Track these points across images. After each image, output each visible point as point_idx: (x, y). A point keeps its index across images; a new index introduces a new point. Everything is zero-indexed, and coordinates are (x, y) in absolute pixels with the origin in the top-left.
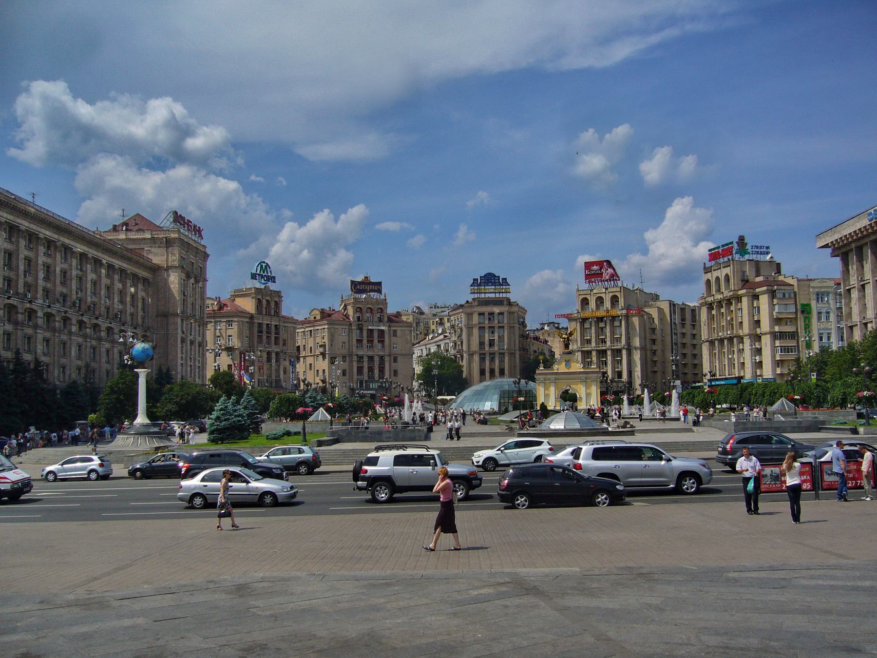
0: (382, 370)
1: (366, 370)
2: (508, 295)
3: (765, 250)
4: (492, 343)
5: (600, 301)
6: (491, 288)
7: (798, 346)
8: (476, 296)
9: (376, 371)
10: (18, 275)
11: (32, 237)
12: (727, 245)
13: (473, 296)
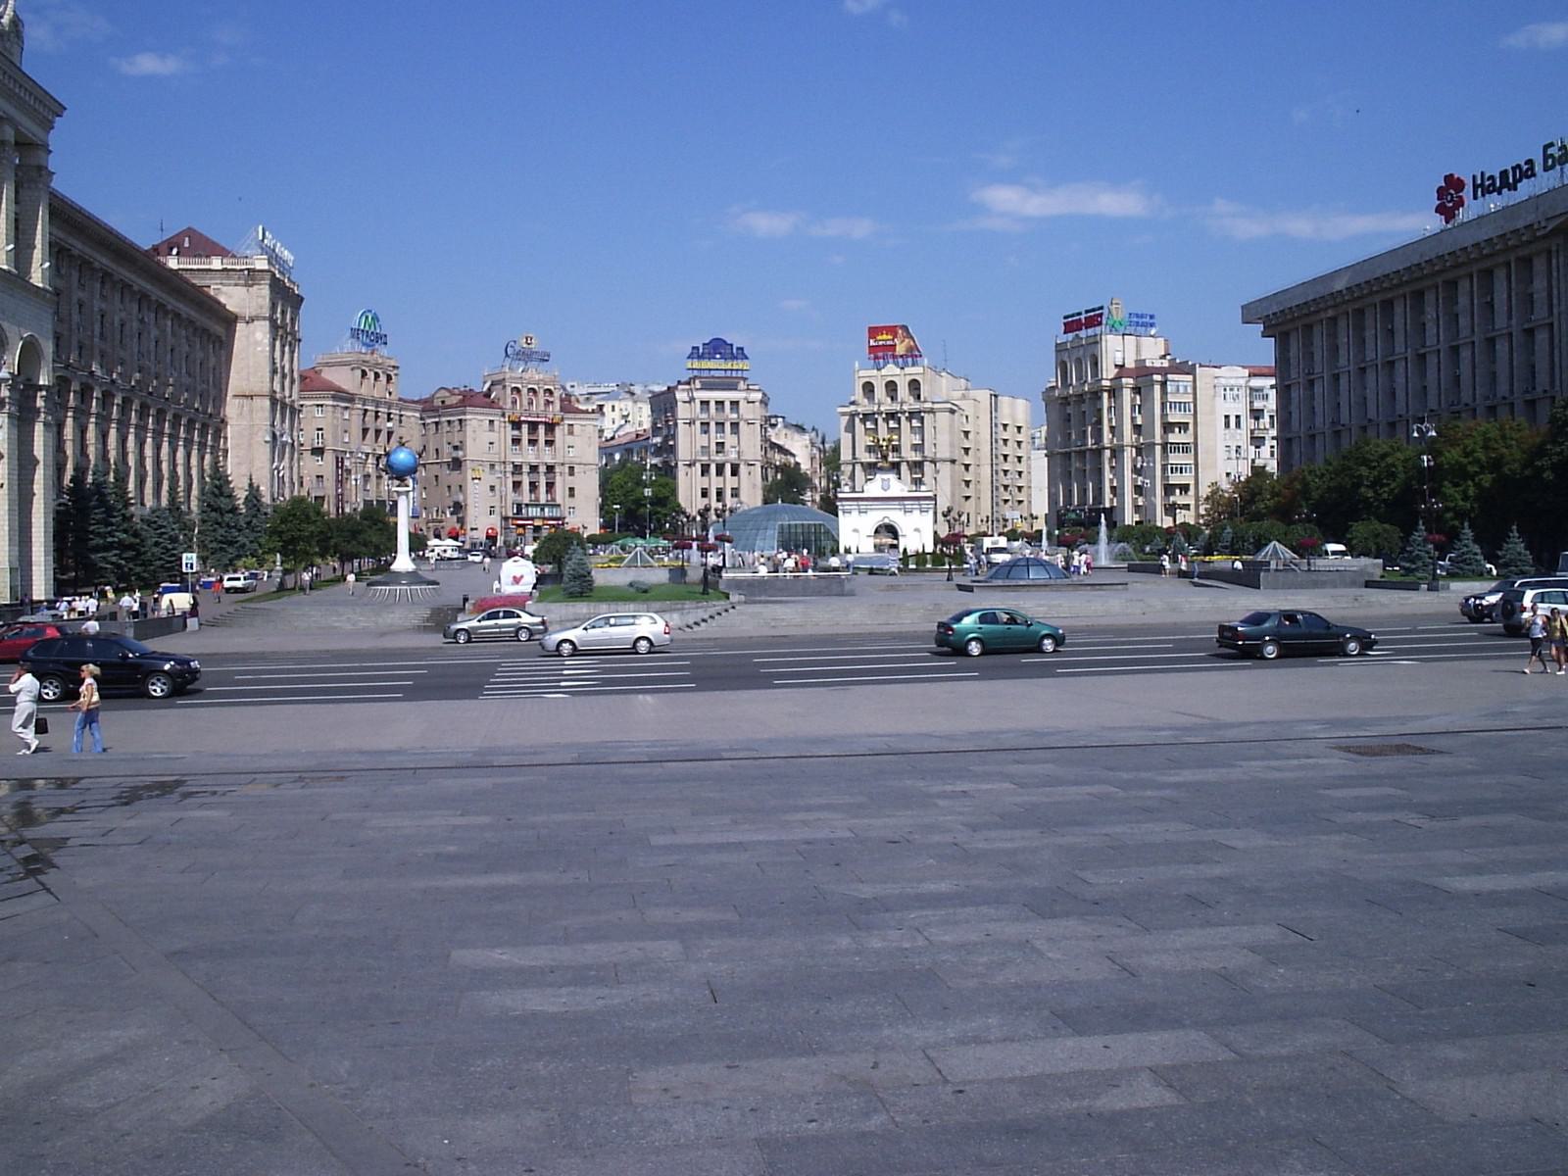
0: (550, 486)
1: (526, 486)
3: (1148, 320)
4: (720, 445)
7: (1196, 465)
9: (543, 488)
10: (70, 330)
12: (1093, 310)
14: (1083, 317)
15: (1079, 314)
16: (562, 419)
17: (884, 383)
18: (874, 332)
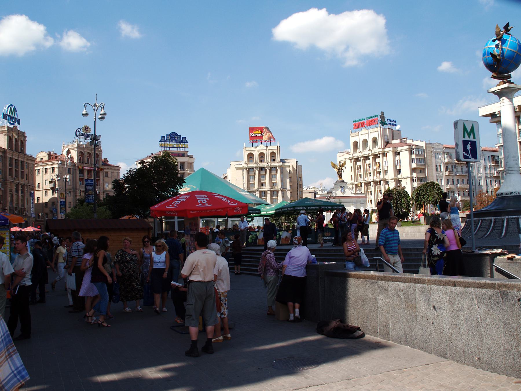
2: (187, 150)
3: (394, 123)
5: (262, 156)
6: (174, 144)
8: (163, 149)
12: (371, 117)
13: (160, 149)
14: (365, 121)
15: (363, 119)
16: (103, 169)
17: (258, 154)
18: (252, 130)
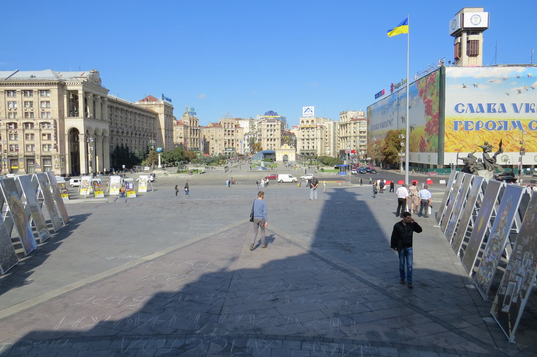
0: (233, 144)
11: (122, 110)
